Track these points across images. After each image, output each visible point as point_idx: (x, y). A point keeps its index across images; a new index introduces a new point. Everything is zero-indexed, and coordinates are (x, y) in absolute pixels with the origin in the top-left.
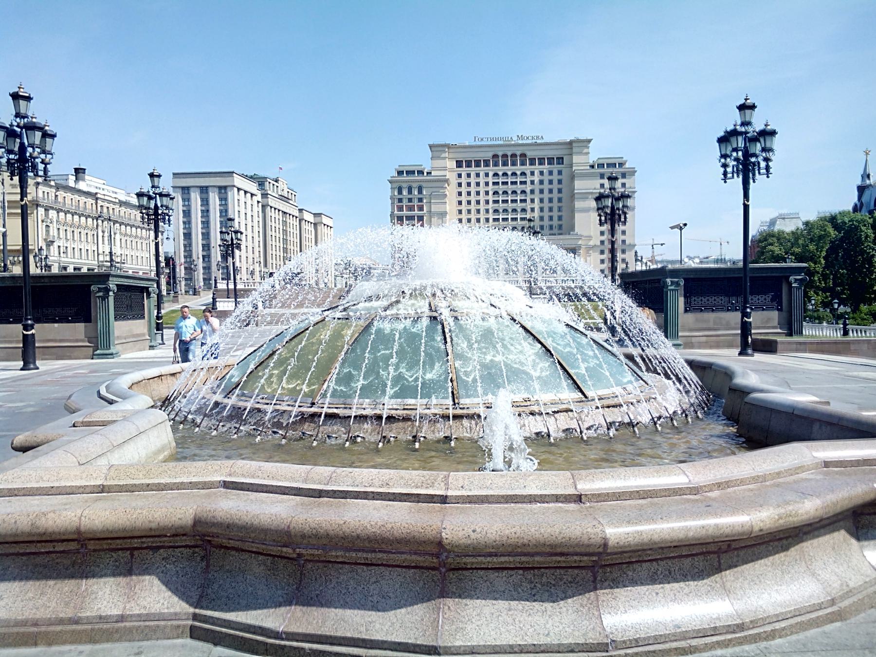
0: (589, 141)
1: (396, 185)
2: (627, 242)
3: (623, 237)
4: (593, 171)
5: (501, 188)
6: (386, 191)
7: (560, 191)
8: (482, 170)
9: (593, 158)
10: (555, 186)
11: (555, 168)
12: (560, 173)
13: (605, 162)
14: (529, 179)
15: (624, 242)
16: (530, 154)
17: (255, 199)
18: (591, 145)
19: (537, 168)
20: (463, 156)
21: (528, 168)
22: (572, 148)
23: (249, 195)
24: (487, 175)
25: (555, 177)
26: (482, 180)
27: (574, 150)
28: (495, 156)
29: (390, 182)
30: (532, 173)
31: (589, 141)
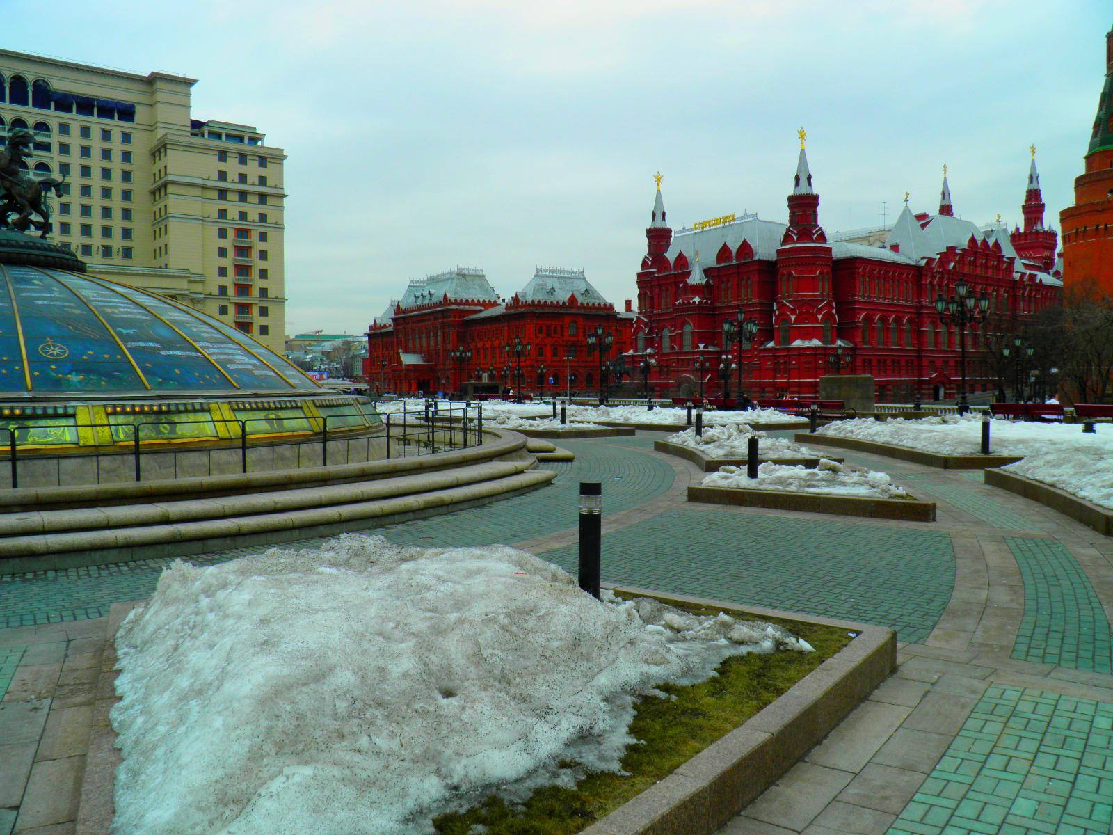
0: (190, 83)
2: (271, 294)
3: (262, 283)
7: (127, 176)
11: (116, 126)
12: (126, 138)
14: (55, 139)
15: (264, 292)
16: (59, 84)
18: (193, 89)
19: (75, 120)
21: (53, 117)
22: (153, 93)
27: (160, 96)
30: (64, 129)
31: (190, 83)
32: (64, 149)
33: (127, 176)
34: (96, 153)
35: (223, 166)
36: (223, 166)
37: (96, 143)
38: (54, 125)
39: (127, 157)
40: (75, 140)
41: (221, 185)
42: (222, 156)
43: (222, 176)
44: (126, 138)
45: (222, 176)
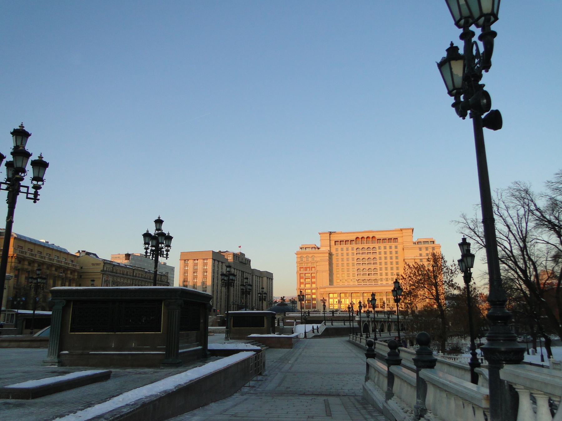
1: (299, 256)
4: (415, 246)
5: (361, 257)
6: (294, 259)
8: (349, 246)
9: (415, 240)
10: (394, 255)
11: (393, 245)
12: (396, 247)
13: (422, 240)
16: (378, 237)
17: (224, 265)
19: (382, 245)
20: (339, 238)
21: (376, 245)
23: (220, 264)
24: (353, 249)
25: (394, 250)
26: (350, 251)
28: (357, 238)
29: (297, 254)
30: (379, 248)
32: (380, 253)
33: (397, 258)
34: (388, 253)
35: (420, 252)
36: (420, 252)
37: (388, 250)
38: (377, 247)
39: (396, 252)
40: (382, 250)
41: (421, 258)
42: (420, 249)
43: (421, 255)
44: (396, 247)
45: (421, 255)
